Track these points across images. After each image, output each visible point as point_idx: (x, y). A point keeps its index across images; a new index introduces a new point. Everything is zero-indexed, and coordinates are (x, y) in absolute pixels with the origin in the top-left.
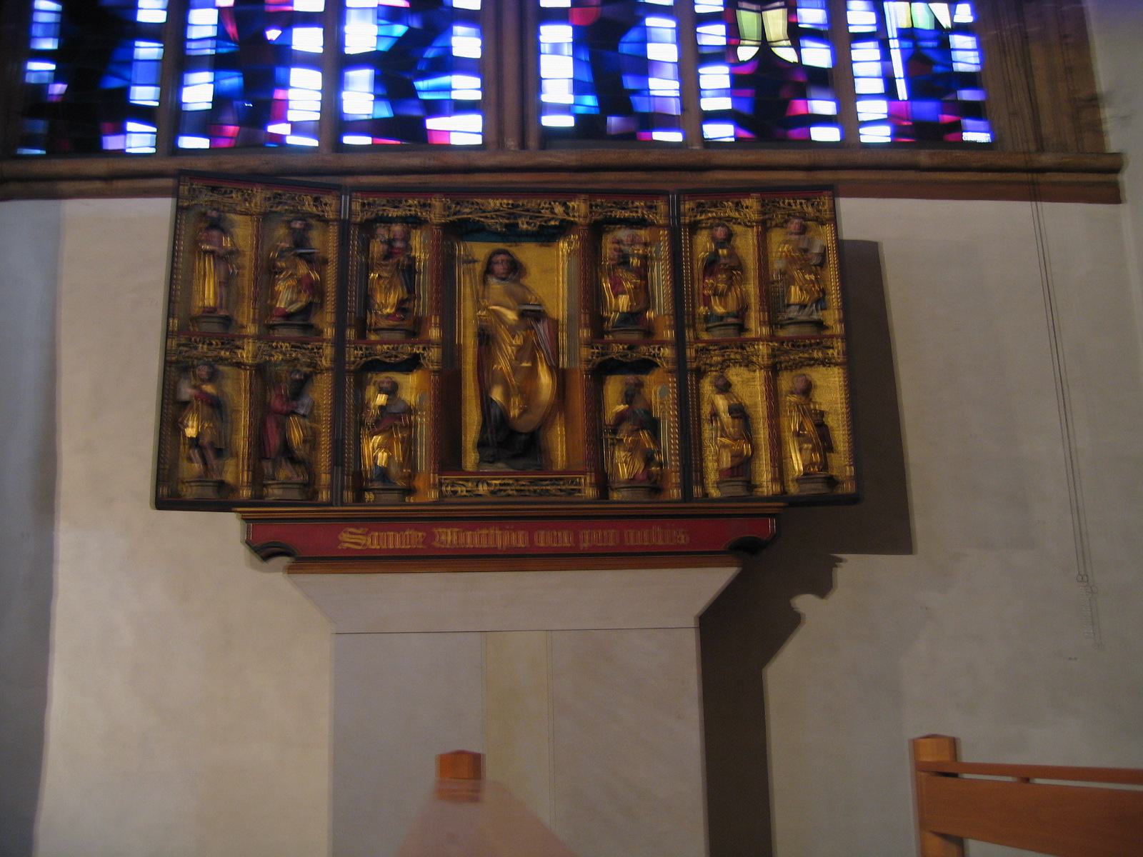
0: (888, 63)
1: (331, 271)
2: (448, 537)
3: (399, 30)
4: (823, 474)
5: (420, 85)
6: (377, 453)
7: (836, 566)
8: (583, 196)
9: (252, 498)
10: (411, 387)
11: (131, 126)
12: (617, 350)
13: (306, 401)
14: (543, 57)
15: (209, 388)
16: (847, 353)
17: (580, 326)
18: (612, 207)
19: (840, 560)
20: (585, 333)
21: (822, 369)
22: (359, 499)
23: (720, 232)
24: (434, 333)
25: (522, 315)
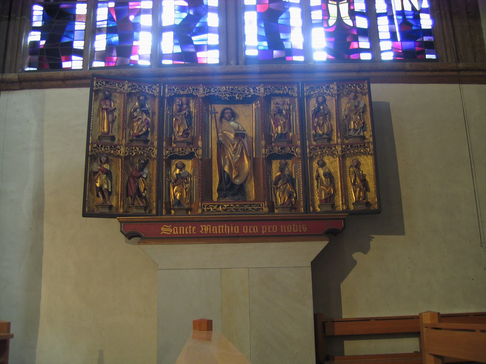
0: (393, 26)
1: (156, 117)
2: (206, 229)
3: (184, 15)
4: (365, 201)
5: (194, 38)
6: (175, 192)
8: (262, 85)
10: (189, 164)
11: (74, 58)
12: (276, 149)
13: (146, 171)
15: (106, 166)
16: (375, 149)
17: (262, 140)
18: (275, 89)
19: (374, 238)
20: (263, 143)
21: (365, 157)
22: (169, 212)
23: (320, 99)
24: (200, 143)
25: (236, 135)
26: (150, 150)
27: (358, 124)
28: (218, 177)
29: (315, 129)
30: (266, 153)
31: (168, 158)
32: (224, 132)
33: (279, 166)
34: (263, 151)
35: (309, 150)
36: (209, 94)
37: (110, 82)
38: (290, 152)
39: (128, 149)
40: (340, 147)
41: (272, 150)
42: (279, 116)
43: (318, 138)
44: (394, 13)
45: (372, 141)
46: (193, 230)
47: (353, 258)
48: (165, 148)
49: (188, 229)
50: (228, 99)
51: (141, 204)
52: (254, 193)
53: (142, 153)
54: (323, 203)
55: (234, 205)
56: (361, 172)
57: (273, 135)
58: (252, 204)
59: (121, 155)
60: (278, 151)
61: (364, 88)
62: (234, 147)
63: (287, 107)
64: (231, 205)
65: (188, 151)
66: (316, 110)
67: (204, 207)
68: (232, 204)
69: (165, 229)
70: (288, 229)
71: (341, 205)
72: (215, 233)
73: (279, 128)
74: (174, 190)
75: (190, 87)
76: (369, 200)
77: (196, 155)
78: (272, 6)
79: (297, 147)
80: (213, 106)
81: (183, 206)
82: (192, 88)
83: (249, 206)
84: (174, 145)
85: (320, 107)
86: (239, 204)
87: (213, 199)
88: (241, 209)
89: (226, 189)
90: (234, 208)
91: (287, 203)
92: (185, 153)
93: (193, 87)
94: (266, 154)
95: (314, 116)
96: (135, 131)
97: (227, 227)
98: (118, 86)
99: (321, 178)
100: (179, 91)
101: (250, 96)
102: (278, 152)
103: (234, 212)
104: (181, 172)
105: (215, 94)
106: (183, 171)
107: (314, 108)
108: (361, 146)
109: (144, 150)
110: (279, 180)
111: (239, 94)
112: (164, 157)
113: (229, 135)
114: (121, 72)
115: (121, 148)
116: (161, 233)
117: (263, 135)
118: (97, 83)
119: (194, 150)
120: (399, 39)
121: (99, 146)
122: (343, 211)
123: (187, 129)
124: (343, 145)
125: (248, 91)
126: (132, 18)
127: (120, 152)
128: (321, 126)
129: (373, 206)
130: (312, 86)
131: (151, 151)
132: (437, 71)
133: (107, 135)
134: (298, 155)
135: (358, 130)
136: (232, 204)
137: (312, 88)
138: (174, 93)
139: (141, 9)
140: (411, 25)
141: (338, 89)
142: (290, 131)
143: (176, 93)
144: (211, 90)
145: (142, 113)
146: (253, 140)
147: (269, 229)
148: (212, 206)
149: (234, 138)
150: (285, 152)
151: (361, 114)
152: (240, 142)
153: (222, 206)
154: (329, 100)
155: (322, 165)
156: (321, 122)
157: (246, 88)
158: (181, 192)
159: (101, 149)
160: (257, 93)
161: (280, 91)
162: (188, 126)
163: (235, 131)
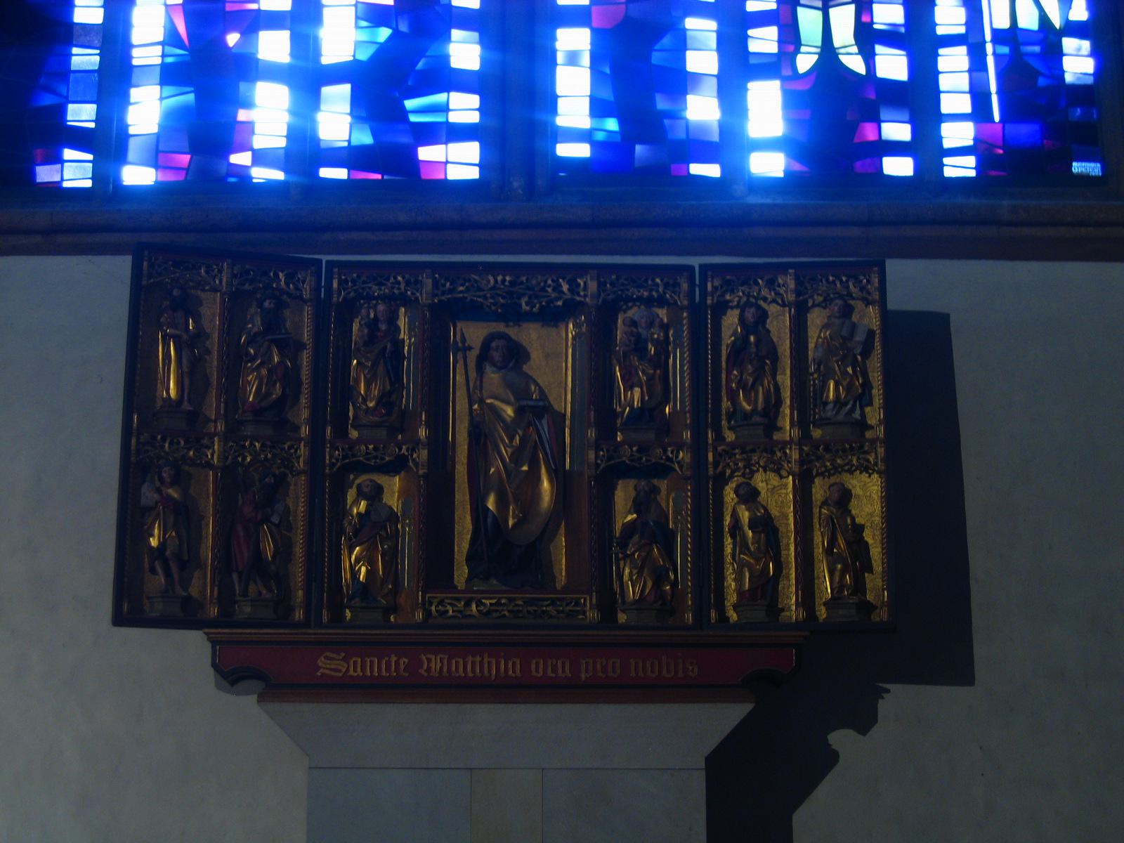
1: (305, 358)
2: (434, 664)
3: (384, 33)
5: (410, 104)
7: (883, 698)
10: (393, 490)
11: (68, 154)
13: (279, 507)
14: (558, 68)
15: (173, 493)
19: (888, 691)
20: (591, 434)
21: (864, 476)
22: (337, 618)
23: (750, 314)
24: (423, 433)
25: (519, 411)
26: (290, 448)
27: (849, 389)
28: (470, 522)
29: (733, 397)
30: (599, 462)
32: (489, 401)
33: (633, 494)
34: (590, 457)
36: (450, 296)
38: (663, 461)
39: (232, 446)
40: (797, 451)
42: (636, 359)
44: (988, 36)
45: (882, 436)
46: (402, 667)
47: (830, 745)
48: (330, 443)
49: (388, 664)
50: (499, 311)
52: (564, 567)
53: (269, 456)
55: (511, 600)
56: (849, 521)
57: (619, 409)
58: (561, 600)
62: (514, 444)
64: (503, 601)
67: (431, 604)
68: (506, 598)
71: (794, 608)
72: (457, 675)
73: (637, 391)
74: (353, 557)
76: (870, 597)
78: (635, 10)
79: (680, 446)
80: (459, 325)
82: (403, 278)
83: (548, 605)
84: (354, 434)
85: (746, 340)
86: (522, 598)
87: (455, 583)
88: (529, 612)
90: (510, 608)
92: (383, 459)
93: (407, 276)
94: (597, 466)
96: (252, 396)
98: (207, 272)
99: (743, 531)
100: (370, 285)
102: (629, 460)
105: (466, 295)
107: (733, 338)
108: (852, 448)
110: (631, 537)
111: (530, 297)
112: (328, 468)
113: (502, 409)
114: (207, 216)
115: (213, 442)
116: (319, 674)
118: (151, 265)
119: (407, 451)
120: (997, 118)
121: (154, 438)
122: (797, 625)
124: (806, 446)
125: (554, 290)
126: (232, 39)
127: (212, 455)
128: (749, 390)
129: (878, 611)
130: (728, 277)
131: (292, 451)
134: (684, 469)
135: (846, 404)
136: (506, 598)
137: (728, 282)
138: (356, 291)
139: (259, 10)
140: (1036, 74)
142: (667, 402)
143: (360, 290)
145: (269, 348)
146: (565, 422)
147: (599, 666)
148: (453, 602)
149: (513, 420)
150: (650, 460)
151: (859, 357)
153: (479, 603)
154: (775, 315)
155: (749, 496)
156: (751, 380)
157: (550, 282)
158: (371, 562)
159: (163, 447)
160: (579, 295)
161: (642, 291)
162: (392, 384)
163: (518, 399)
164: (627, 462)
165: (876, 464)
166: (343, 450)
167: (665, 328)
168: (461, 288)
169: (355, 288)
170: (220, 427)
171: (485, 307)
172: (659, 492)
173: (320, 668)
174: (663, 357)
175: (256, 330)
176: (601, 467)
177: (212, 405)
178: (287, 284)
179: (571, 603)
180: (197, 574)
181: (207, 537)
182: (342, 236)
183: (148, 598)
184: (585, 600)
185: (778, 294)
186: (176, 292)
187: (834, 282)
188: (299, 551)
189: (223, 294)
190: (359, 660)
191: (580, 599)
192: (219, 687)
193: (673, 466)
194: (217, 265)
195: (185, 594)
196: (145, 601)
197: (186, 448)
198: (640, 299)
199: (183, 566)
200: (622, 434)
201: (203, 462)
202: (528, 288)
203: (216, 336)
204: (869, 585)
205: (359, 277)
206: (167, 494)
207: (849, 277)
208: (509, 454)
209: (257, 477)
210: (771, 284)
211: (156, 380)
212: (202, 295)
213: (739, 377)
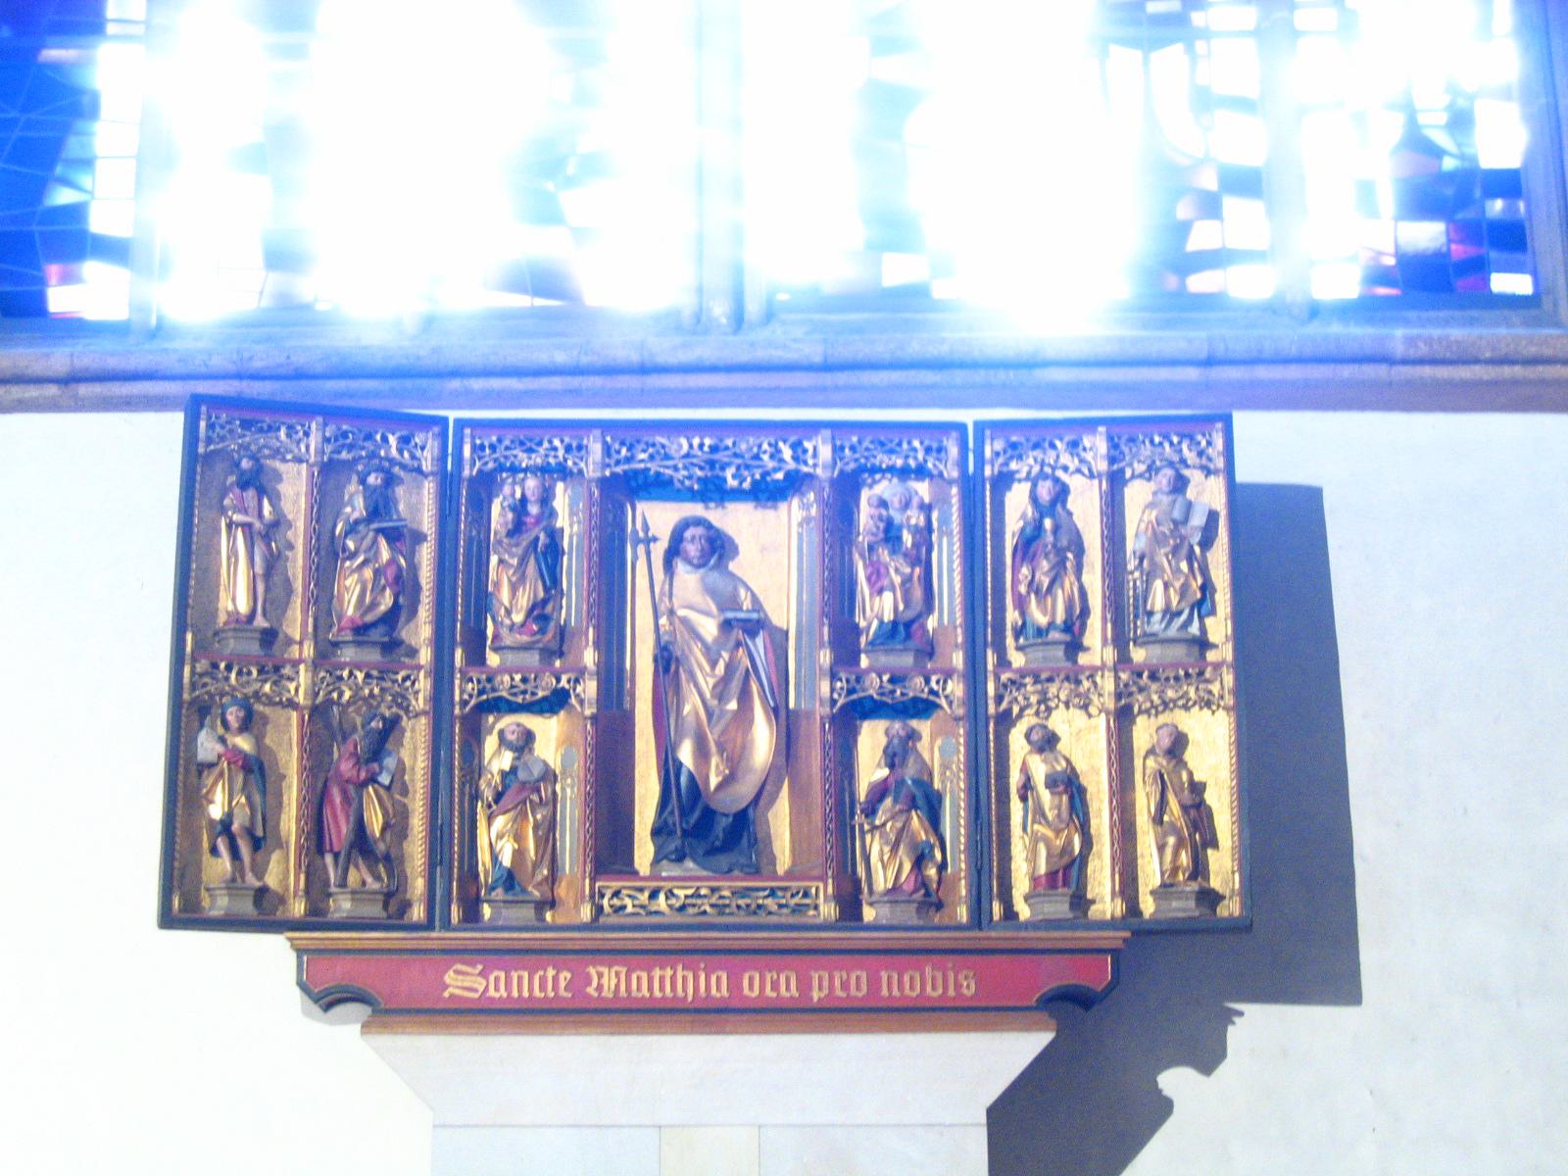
1: (426, 554)
2: (607, 980)
7: (1233, 1023)
8: (827, 433)
9: (306, 915)
10: (550, 736)
12: (873, 686)
13: (390, 762)
15: (244, 743)
17: (822, 645)
19: (1240, 1014)
20: (825, 657)
22: (472, 915)
23: (1045, 490)
24: (589, 657)
25: (726, 626)
26: (405, 679)
27: (1184, 591)
29: (1021, 604)
30: (836, 696)
31: (471, 709)
32: (681, 612)
33: (884, 741)
34: (822, 690)
35: (997, 689)
36: (626, 467)
37: (257, 422)
39: (324, 678)
40: (1112, 680)
41: (858, 687)
42: (886, 552)
43: (1031, 641)
45: (1229, 657)
46: (562, 984)
48: (461, 671)
51: (372, 884)
53: (376, 691)
54: (1041, 890)
55: (713, 890)
56: (1185, 776)
57: (863, 624)
58: (785, 889)
59: (301, 699)
60: (880, 691)
61: (1210, 450)
63: (916, 518)
64: (703, 892)
65: (547, 684)
66: (1028, 530)
67: (602, 896)
68: (706, 887)
69: (457, 980)
70: (907, 986)
71: (1108, 898)
72: (640, 995)
73: (888, 596)
75: (555, 436)
76: (1215, 883)
77: (573, 700)
79: (948, 674)
81: (524, 891)
84: (493, 659)
86: (730, 887)
88: (739, 907)
89: (684, 831)
90: (714, 900)
91: (909, 887)
92: (533, 694)
94: (833, 702)
95: (1019, 554)
97: (686, 973)
98: (289, 435)
101: (780, 476)
102: (878, 694)
103: (710, 915)
104: (517, 763)
105: (649, 465)
106: (526, 757)
108: (1187, 675)
109: (383, 679)
110: (881, 799)
111: (738, 468)
114: (288, 357)
115: (297, 673)
116: (446, 994)
117: (826, 630)
118: (211, 426)
119: (569, 681)
121: (215, 666)
122: (1112, 924)
123: (545, 602)
124: (1124, 671)
125: (772, 456)
127: (297, 690)
128: (1043, 594)
129: (1226, 902)
131: (408, 683)
132: (1512, 362)
133: (249, 627)
135: (1179, 613)
136: (706, 887)
137: (1014, 446)
138: (495, 460)
140: (1438, 153)
141: (1112, 452)
144: (634, 451)
145: (375, 541)
147: (837, 983)
149: (716, 640)
151: (1197, 550)
152: (738, 651)
153: (670, 894)
155: (1046, 743)
156: (1046, 582)
157: (765, 446)
158: (518, 837)
159: (227, 679)
161: (894, 457)
162: (546, 589)
163: (722, 609)
164: (875, 696)
165: (1222, 697)
166: (479, 681)
167: (926, 509)
168: (642, 456)
169: (495, 456)
170: (308, 650)
171: (676, 481)
172: (920, 738)
173: (446, 987)
174: (924, 549)
175: (356, 515)
176: (839, 704)
177: (296, 622)
178: (400, 451)
179: (798, 893)
180: (276, 856)
181: (289, 804)
182: (477, 384)
183: (208, 890)
184: (817, 889)
185: (1082, 461)
186: (245, 464)
187: (1161, 444)
188: (418, 823)
189: (310, 466)
190: (502, 975)
191: (811, 887)
192: (306, 1013)
193: (937, 700)
194: (303, 426)
195: (258, 884)
196: (204, 894)
197: (261, 681)
198: (891, 469)
199: (257, 844)
200: (868, 657)
201: (284, 699)
202: (736, 455)
203: (300, 525)
204: (1213, 866)
205: (500, 441)
206: (234, 746)
207: (1182, 436)
208: (711, 686)
209: (359, 721)
210: (1074, 445)
211: (218, 586)
212: (278, 465)
213: (1030, 578)
